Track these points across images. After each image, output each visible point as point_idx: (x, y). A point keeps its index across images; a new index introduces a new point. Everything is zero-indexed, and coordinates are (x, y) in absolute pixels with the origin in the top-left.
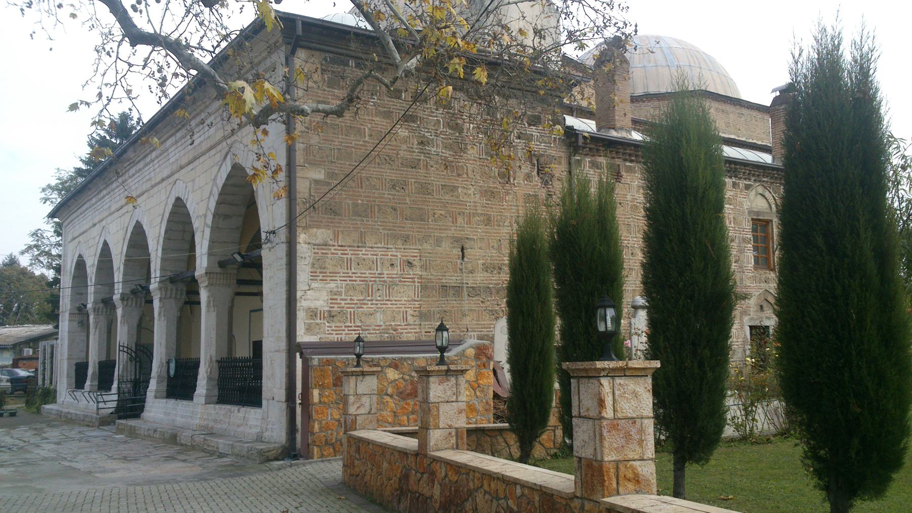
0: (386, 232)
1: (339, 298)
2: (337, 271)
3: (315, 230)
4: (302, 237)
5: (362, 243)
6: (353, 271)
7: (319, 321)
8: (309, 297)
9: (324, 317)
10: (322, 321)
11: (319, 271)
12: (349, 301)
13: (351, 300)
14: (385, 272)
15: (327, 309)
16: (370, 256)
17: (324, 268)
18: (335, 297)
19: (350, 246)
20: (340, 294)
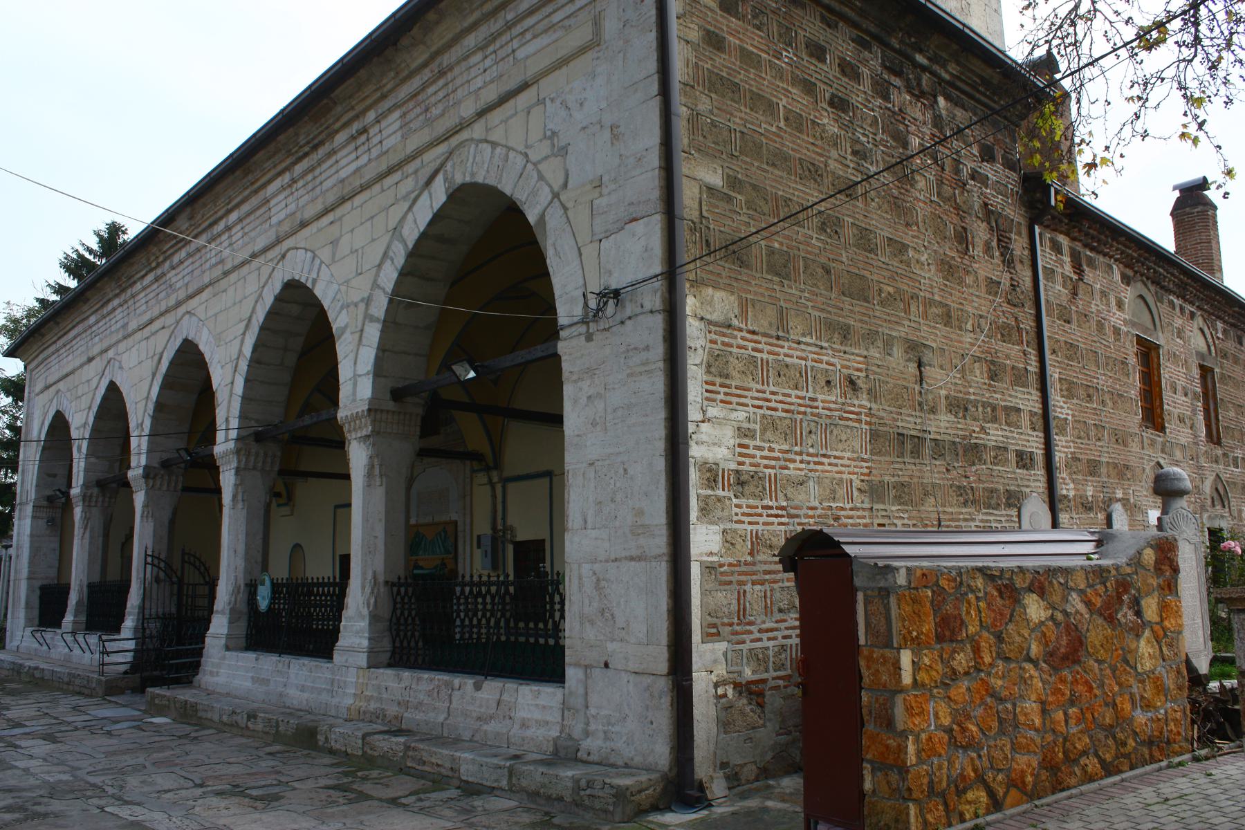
0: (817, 314)
1: (752, 443)
2: (746, 385)
3: (710, 291)
4: (691, 304)
5: (780, 333)
6: (773, 388)
7: (720, 493)
8: (704, 438)
9: (729, 485)
10: (726, 493)
11: (718, 380)
12: (766, 453)
13: (771, 450)
14: (820, 397)
15: (733, 466)
17: (727, 376)
18: (746, 441)
19: (765, 335)
20: (753, 437)
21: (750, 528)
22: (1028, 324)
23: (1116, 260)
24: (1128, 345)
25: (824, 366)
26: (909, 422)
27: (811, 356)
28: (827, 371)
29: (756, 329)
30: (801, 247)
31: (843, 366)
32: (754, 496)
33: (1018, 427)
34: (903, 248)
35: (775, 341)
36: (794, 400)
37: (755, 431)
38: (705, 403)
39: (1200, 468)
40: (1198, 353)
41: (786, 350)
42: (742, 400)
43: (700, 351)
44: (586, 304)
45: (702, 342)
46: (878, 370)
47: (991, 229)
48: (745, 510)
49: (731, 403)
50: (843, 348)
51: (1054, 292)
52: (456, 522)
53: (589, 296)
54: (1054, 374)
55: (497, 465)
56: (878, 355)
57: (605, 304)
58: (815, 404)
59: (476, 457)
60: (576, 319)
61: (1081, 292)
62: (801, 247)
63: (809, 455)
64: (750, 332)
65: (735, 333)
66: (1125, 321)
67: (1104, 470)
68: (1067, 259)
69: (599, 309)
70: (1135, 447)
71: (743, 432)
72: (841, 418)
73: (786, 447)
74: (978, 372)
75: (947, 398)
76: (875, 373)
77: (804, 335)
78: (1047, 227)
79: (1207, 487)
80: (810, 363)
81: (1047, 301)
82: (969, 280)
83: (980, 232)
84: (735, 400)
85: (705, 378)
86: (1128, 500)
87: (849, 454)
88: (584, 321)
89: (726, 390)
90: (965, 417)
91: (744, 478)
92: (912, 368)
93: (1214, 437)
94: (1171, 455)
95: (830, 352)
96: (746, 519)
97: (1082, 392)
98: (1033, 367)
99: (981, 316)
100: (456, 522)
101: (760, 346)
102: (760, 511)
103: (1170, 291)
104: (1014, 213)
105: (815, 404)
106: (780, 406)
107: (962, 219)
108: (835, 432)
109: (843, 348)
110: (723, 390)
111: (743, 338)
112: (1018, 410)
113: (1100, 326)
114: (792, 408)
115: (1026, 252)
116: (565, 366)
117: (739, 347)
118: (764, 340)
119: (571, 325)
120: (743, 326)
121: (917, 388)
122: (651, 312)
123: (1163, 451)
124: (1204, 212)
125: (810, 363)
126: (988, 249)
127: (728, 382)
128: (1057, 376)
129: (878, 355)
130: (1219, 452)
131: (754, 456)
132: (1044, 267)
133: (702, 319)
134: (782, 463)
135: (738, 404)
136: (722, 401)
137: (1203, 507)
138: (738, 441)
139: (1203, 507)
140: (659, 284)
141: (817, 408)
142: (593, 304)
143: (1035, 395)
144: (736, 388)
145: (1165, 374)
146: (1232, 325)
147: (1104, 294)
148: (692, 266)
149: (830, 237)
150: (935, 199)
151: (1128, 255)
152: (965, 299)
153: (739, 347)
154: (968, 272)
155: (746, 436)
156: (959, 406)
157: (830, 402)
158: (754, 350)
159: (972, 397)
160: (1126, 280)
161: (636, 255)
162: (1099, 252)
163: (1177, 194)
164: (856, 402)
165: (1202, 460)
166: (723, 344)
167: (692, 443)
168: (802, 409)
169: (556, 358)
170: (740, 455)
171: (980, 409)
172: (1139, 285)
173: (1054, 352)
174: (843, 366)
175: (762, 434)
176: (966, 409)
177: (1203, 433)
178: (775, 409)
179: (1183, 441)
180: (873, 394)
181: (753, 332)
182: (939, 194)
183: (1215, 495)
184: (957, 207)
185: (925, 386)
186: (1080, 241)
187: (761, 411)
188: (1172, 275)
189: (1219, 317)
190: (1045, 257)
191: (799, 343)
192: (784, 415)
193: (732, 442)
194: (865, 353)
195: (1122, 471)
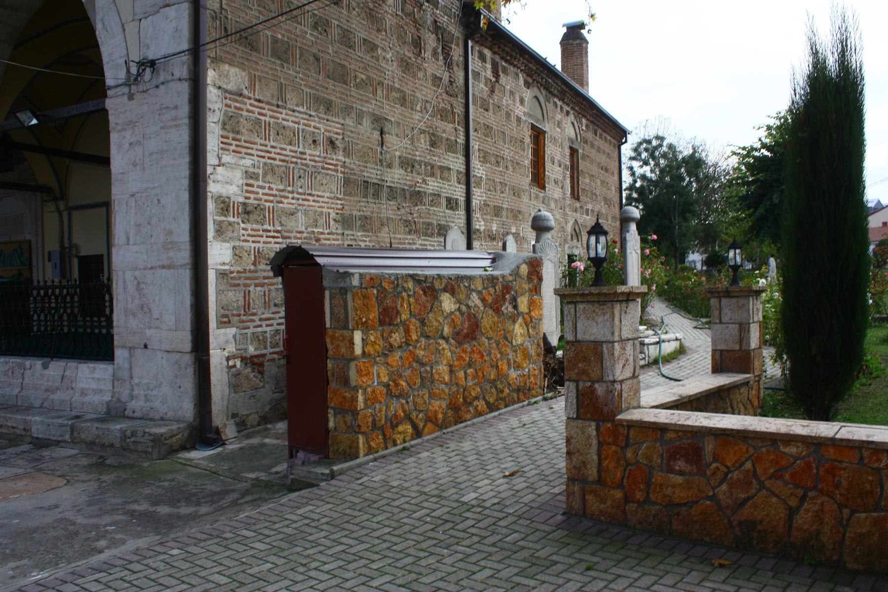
0: (308, 90)
1: (256, 183)
2: (252, 140)
3: (227, 67)
4: (211, 75)
5: (280, 102)
7: (231, 219)
8: (219, 178)
9: (238, 213)
10: (235, 220)
11: (231, 135)
12: (266, 191)
13: (270, 189)
14: (308, 152)
15: (242, 200)
16: (291, 124)
17: (238, 133)
18: (251, 182)
19: (268, 103)
20: (257, 179)
21: (253, 245)
22: (459, 110)
23: (521, 70)
24: (525, 129)
25: (312, 129)
26: (372, 173)
27: (302, 121)
28: (314, 133)
29: (262, 98)
30: (298, 39)
31: (326, 130)
32: (257, 222)
33: (449, 181)
34: (373, 47)
35: (275, 109)
36: (288, 153)
37: (258, 174)
38: (221, 152)
39: (565, 214)
40: (569, 139)
41: (283, 116)
42: (249, 151)
43: (217, 112)
44: (128, 71)
45: (219, 105)
46: (352, 135)
47: (438, 39)
48: (250, 232)
49: (240, 153)
50: (326, 117)
51: (478, 88)
52: (30, 241)
53: (132, 64)
54: (475, 145)
55: (64, 197)
56: (351, 124)
57: (144, 70)
58: (304, 157)
59: (45, 190)
60: (120, 82)
61: (497, 90)
62: (298, 39)
63: (298, 193)
64: (256, 100)
65: (246, 100)
66: (524, 113)
67: (504, 213)
68: (489, 66)
69: (139, 75)
70: (525, 199)
71: (249, 175)
72: (323, 168)
73: (281, 187)
74: (423, 141)
75: (400, 157)
76: (349, 137)
77: (297, 105)
78: (477, 42)
79: (569, 228)
80: (301, 127)
81: (473, 95)
82: (420, 75)
83: (430, 41)
84: (244, 150)
85: (221, 133)
86: (519, 234)
87: (328, 194)
88: (127, 84)
89: (237, 143)
90: (412, 172)
91: (249, 208)
92: (376, 135)
93: (575, 196)
94: (548, 205)
95: (317, 119)
96: (251, 239)
97: (493, 159)
98: (461, 140)
99: (427, 101)
100: (30, 241)
101: (264, 111)
102: (261, 233)
103: (554, 95)
104: (455, 30)
105: (304, 157)
106: (278, 157)
107: (418, 30)
108: (318, 178)
109: (326, 117)
110: (234, 143)
111: (251, 105)
112: (449, 169)
113: (508, 115)
114: (287, 158)
115: (461, 59)
116: (112, 119)
117: (248, 111)
118: (267, 107)
119: (116, 86)
120: (252, 95)
121: (379, 149)
122: (180, 80)
123: (543, 202)
124: (580, 45)
125: (301, 127)
126: (435, 53)
127: (238, 137)
128: (477, 147)
129: (351, 124)
130: (578, 205)
131: (257, 193)
132: (473, 71)
133: (220, 88)
134: (278, 199)
135: (246, 154)
136: (234, 151)
137: (565, 241)
138: (245, 181)
139: (565, 241)
140: (186, 58)
141: (305, 159)
142: (134, 70)
143: (462, 159)
144: (245, 141)
145: (548, 151)
146: (591, 122)
147: (512, 93)
148: (212, 45)
149: (321, 34)
150: (400, 13)
151: (530, 68)
152: (417, 88)
153: (248, 111)
154: (420, 69)
155: (251, 178)
156: (408, 164)
157: (316, 156)
158: (259, 114)
159: (418, 158)
160: (527, 85)
161: (169, 33)
162: (510, 64)
163: (565, 30)
164: (334, 157)
165: (567, 210)
166: (236, 108)
167: (210, 182)
168: (294, 160)
169: (105, 111)
170: (247, 191)
171: (423, 167)
172: (536, 89)
173: (476, 130)
174: (326, 130)
175: (264, 177)
176: (413, 166)
177: (569, 193)
178: (274, 159)
179: (556, 196)
180: (347, 152)
181: (259, 101)
182: (402, 10)
183: (574, 233)
184: (415, 21)
185: (384, 148)
186: (499, 54)
187: (264, 160)
188: (557, 84)
189: (584, 116)
190: (474, 64)
191: (294, 111)
192: (281, 163)
193: (241, 182)
194: (343, 122)
195: (516, 214)
